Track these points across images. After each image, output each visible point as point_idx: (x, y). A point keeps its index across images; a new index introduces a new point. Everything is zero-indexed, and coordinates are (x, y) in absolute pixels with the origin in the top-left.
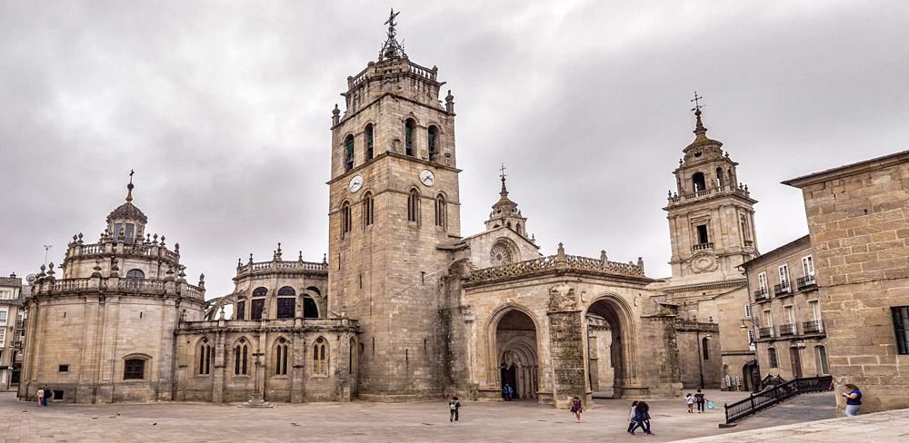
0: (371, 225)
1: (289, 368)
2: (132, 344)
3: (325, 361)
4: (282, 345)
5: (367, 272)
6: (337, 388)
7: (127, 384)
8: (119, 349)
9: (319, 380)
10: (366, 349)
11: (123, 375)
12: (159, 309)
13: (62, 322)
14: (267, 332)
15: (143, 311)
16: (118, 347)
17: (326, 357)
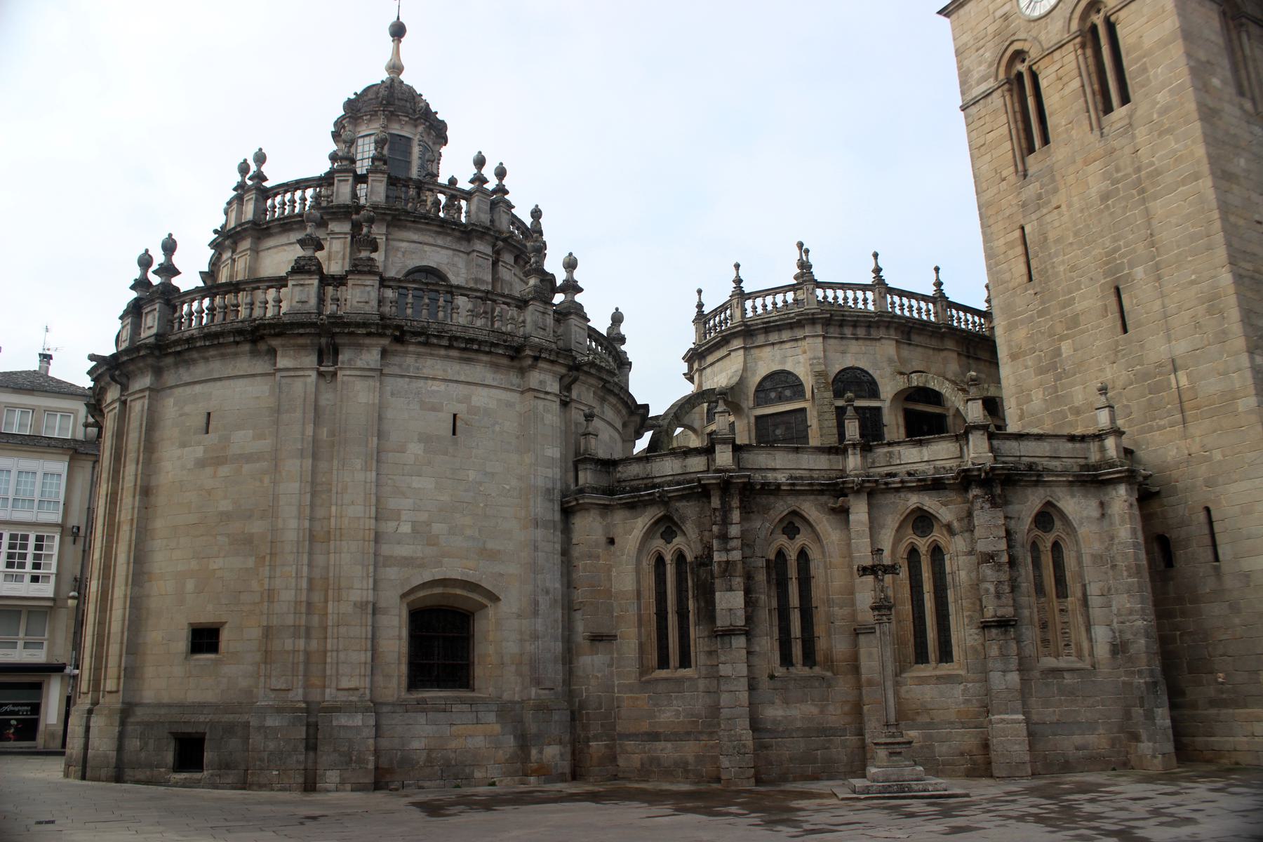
0: (1120, 112)
1: (963, 634)
2: (432, 541)
3: (1072, 601)
4: (923, 544)
5: (1139, 272)
6: (1127, 715)
7: (421, 706)
8: (390, 561)
9: (1068, 679)
10: (1179, 554)
11: (404, 668)
12: (510, 405)
13: (199, 452)
14: (871, 494)
15: (461, 409)
16: (386, 550)
17: (1074, 589)
